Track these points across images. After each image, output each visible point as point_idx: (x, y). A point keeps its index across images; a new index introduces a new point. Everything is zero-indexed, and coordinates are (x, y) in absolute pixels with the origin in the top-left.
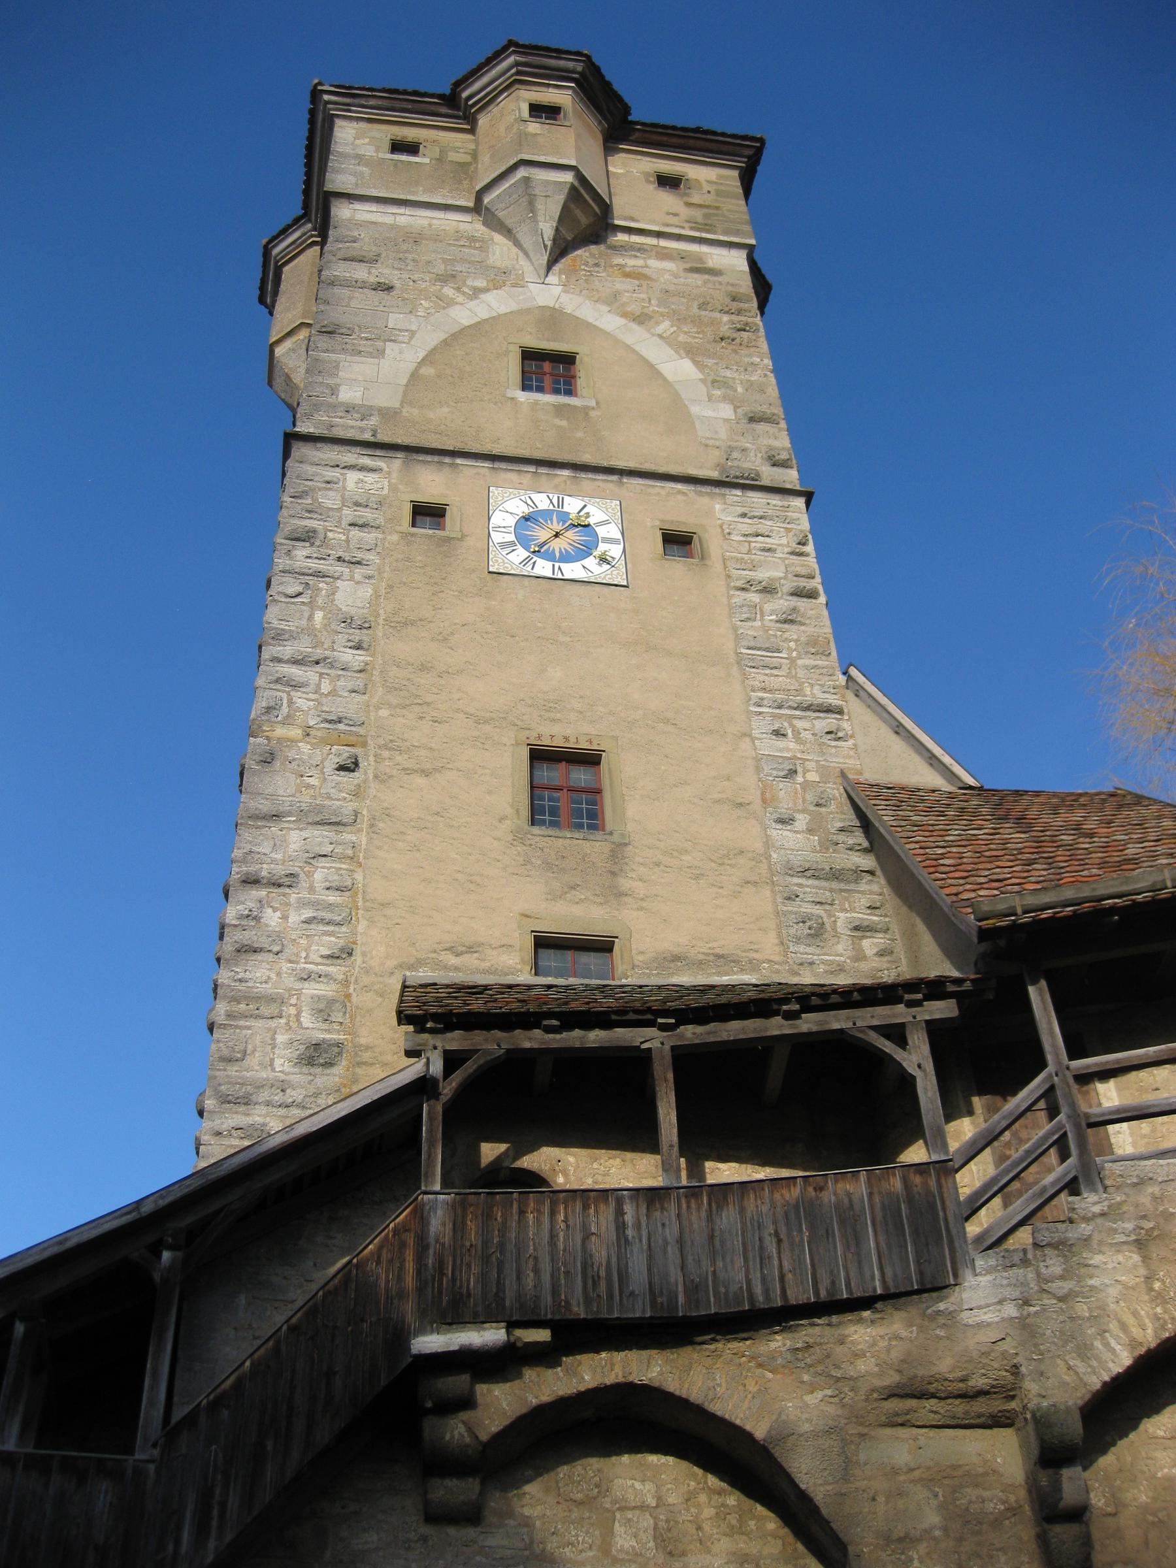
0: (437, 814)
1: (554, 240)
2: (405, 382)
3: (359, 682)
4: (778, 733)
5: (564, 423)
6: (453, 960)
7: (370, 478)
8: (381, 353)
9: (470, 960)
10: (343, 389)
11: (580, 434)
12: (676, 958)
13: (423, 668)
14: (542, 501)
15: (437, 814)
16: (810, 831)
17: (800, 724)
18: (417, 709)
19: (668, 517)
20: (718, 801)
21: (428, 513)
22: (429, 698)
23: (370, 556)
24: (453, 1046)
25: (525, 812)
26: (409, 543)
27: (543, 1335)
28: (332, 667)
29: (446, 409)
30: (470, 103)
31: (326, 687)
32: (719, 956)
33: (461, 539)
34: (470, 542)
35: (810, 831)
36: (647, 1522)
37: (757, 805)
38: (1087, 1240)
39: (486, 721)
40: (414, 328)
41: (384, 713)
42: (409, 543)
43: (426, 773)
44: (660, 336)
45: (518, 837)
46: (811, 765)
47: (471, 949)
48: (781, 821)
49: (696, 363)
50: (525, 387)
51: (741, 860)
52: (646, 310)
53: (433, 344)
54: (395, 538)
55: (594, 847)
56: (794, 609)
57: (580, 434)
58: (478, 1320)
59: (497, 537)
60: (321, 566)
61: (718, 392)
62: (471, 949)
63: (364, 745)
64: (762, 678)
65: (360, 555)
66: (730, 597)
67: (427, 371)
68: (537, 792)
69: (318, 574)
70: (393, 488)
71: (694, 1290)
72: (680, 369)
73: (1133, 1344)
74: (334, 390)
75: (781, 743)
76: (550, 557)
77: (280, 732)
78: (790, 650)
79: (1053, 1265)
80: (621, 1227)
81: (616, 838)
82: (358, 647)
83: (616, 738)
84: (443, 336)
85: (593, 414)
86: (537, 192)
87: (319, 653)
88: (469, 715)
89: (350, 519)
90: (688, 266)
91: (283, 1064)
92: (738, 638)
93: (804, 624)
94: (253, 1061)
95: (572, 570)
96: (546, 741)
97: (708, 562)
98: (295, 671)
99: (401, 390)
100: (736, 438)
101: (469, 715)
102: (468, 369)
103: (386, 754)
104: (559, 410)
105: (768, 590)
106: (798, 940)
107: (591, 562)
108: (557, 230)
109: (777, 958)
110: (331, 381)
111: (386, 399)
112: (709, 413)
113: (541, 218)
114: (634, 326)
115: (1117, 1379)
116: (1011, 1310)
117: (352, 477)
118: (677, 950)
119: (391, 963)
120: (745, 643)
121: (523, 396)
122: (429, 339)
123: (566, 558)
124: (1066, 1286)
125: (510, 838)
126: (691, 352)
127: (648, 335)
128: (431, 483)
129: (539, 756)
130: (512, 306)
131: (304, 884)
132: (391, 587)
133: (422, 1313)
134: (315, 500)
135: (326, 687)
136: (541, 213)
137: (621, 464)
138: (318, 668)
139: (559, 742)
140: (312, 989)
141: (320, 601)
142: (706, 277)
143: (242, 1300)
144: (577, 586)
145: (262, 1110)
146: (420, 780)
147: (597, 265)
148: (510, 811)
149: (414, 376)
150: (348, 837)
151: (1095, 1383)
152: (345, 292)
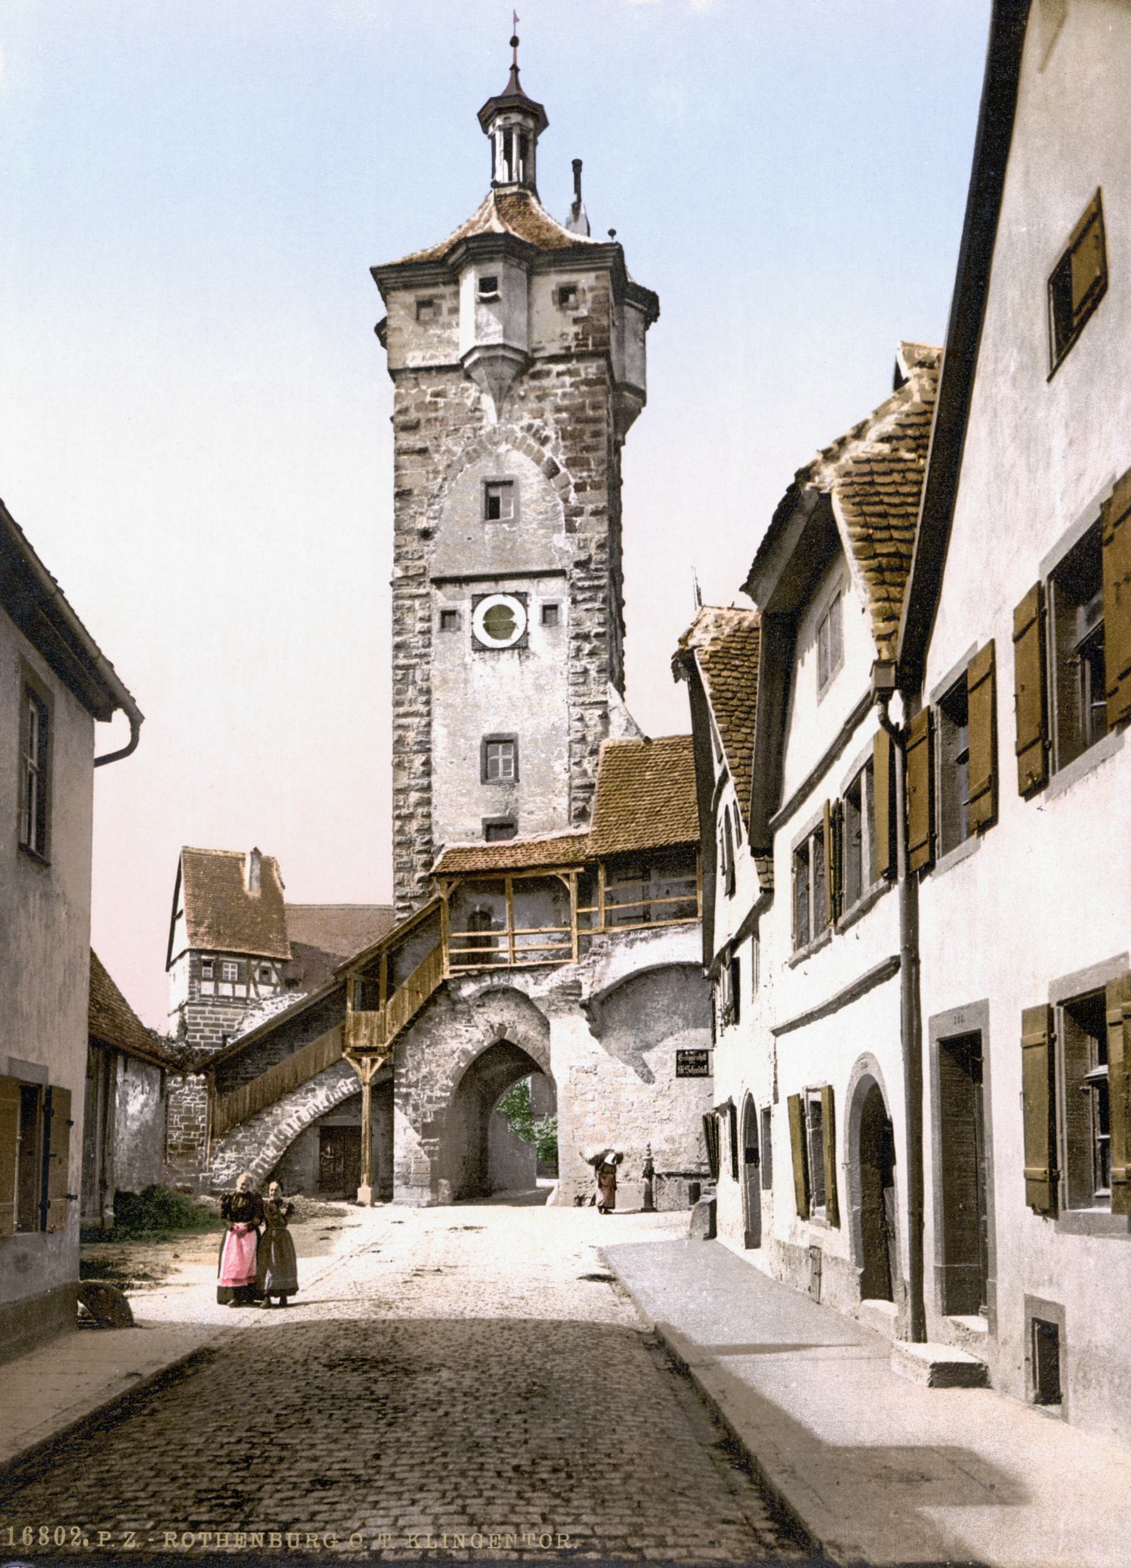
65: (423, 651)
117: (417, 603)
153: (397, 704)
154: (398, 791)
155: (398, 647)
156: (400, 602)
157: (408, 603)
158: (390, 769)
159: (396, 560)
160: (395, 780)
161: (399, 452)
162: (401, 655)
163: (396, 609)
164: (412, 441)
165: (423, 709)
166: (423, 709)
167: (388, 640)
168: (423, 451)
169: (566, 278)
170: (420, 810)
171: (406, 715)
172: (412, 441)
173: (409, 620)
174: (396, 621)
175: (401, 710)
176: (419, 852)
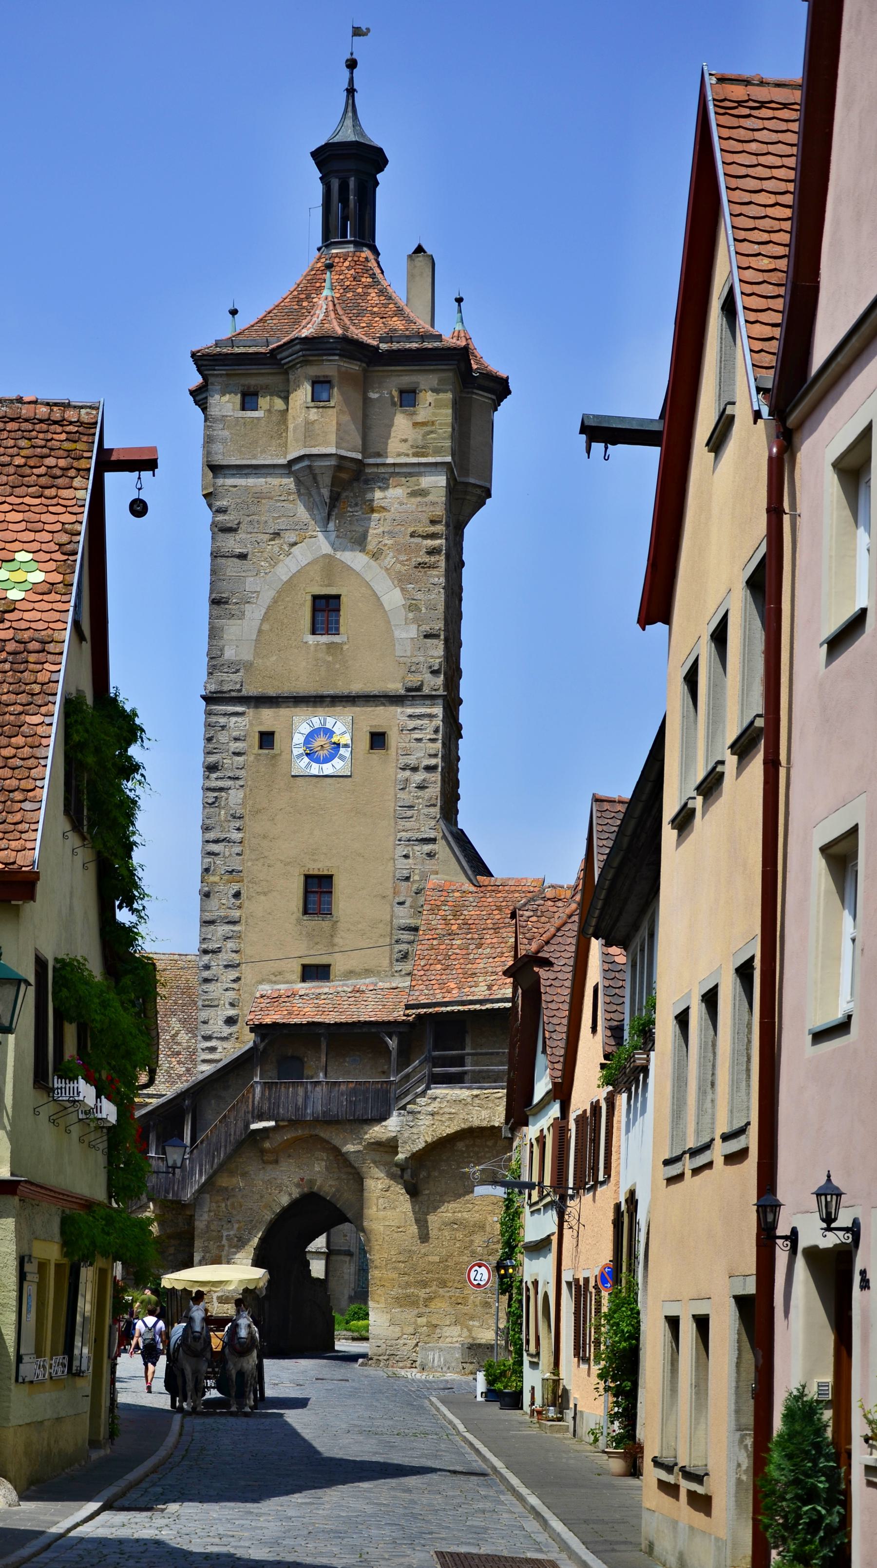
0: (269, 913)
1: (331, 498)
2: (254, 637)
3: (237, 849)
4: (406, 857)
5: (330, 659)
6: (274, 979)
7: (239, 719)
8: (243, 613)
9: (278, 978)
10: (226, 648)
11: (337, 666)
12: (351, 972)
13: (265, 837)
14: (316, 722)
15: (269, 913)
16: (411, 907)
17: (417, 848)
18: (262, 860)
19: (374, 724)
20: (375, 896)
21: (267, 739)
22: (266, 854)
23: (243, 771)
24: (264, 1032)
25: (301, 910)
26: (258, 760)
27: (286, 1123)
28: (229, 842)
29: (274, 658)
30: (283, 362)
31: (227, 854)
32: (366, 970)
33: (280, 755)
34: (284, 756)
35: (411, 907)
36: (324, 1163)
37: (391, 897)
38: (419, 1112)
39: (289, 863)
40: (258, 590)
41: (249, 864)
42: (258, 760)
43: (265, 894)
44: (387, 570)
45: (299, 921)
46: (417, 871)
47: (280, 973)
48: (399, 903)
49: (402, 590)
50: (313, 632)
51: (381, 925)
52: (380, 546)
53: (269, 600)
54: (252, 758)
55: (326, 924)
56: (424, 780)
57: (337, 666)
58: (268, 1120)
59: (296, 752)
60: (220, 784)
61: (411, 615)
62: (280, 973)
63: (242, 881)
64: (403, 823)
65: (238, 773)
66: (397, 774)
67: (266, 627)
68: (309, 895)
69: (221, 789)
70: (251, 724)
71: (324, 1113)
72: (393, 598)
73: (426, 1142)
74: (222, 650)
75: (406, 861)
76: (318, 761)
77: (212, 879)
78: (419, 804)
79: (410, 1118)
80: (306, 1092)
81: (334, 919)
82: (238, 829)
83: (338, 867)
84: (272, 593)
85: (345, 647)
86: (316, 472)
87: (223, 836)
88: (281, 861)
89: (232, 750)
90: (409, 490)
91: (221, 1023)
92: (396, 799)
93: (427, 787)
94: (211, 1022)
95: (328, 769)
96: (311, 872)
97: (389, 752)
98: (215, 848)
99: (253, 643)
100: (415, 653)
101: (281, 861)
102: (285, 621)
103: (251, 885)
104: (330, 646)
105: (415, 769)
106: (397, 961)
107: (336, 760)
108: (331, 491)
109: (387, 969)
110: (221, 643)
111: (246, 654)
112: (404, 635)
113: (321, 486)
114: (372, 562)
115: (420, 1150)
116: (398, 1129)
117: (234, 719)
118: (352, 969)
119: (254, 981)
120: (399, 804)
121: (311, 639)
122: (267, 596)
123: (327, 760)
124: (412, 1124)
125: (295, 922)
126: (401, 581)
127: (379, 570)
128: (268, 718)
129: (309, 878)
130: (309, 558)
131: (224, 950)
132: (251, 790)
133: (253, 1117)
134: (218, 741)
135: (227, 854)
136: (321, 483)
137: (356, 688)
138: (224, 844)
139: (316, 872)
140: (228, 993)
141: (223, 804)
142: (419, 499)
143: (213, 1102)
144: (328, 779)
145: (214, 1040)
146: (262, 898)
147: (356, 505)
148: (296, 910)
149: (260, 631)
150: (236, 928)
151: (415, 1150)
152: (223, 561)
153: (206, 829)
154: (207, 923)
155: (211, 768)
156: (213, 719)
157: (222, 720)
158: (198, 898)
159: (210, 674)
160: (202, 910)
161: (215, 555)
162: (214, 776)
163: (208, 725)
164: (231, 543)
165: (236, 836)
166: (236, 836)
167: (198, 760)
168: (243, 557)
169: (406, 380)
170: (230, 945)
171: (217, 841)
172: (231, 543)
173: (223, 737)
174: (209, 740)
175: (212, 836)
176: (227, 990)
